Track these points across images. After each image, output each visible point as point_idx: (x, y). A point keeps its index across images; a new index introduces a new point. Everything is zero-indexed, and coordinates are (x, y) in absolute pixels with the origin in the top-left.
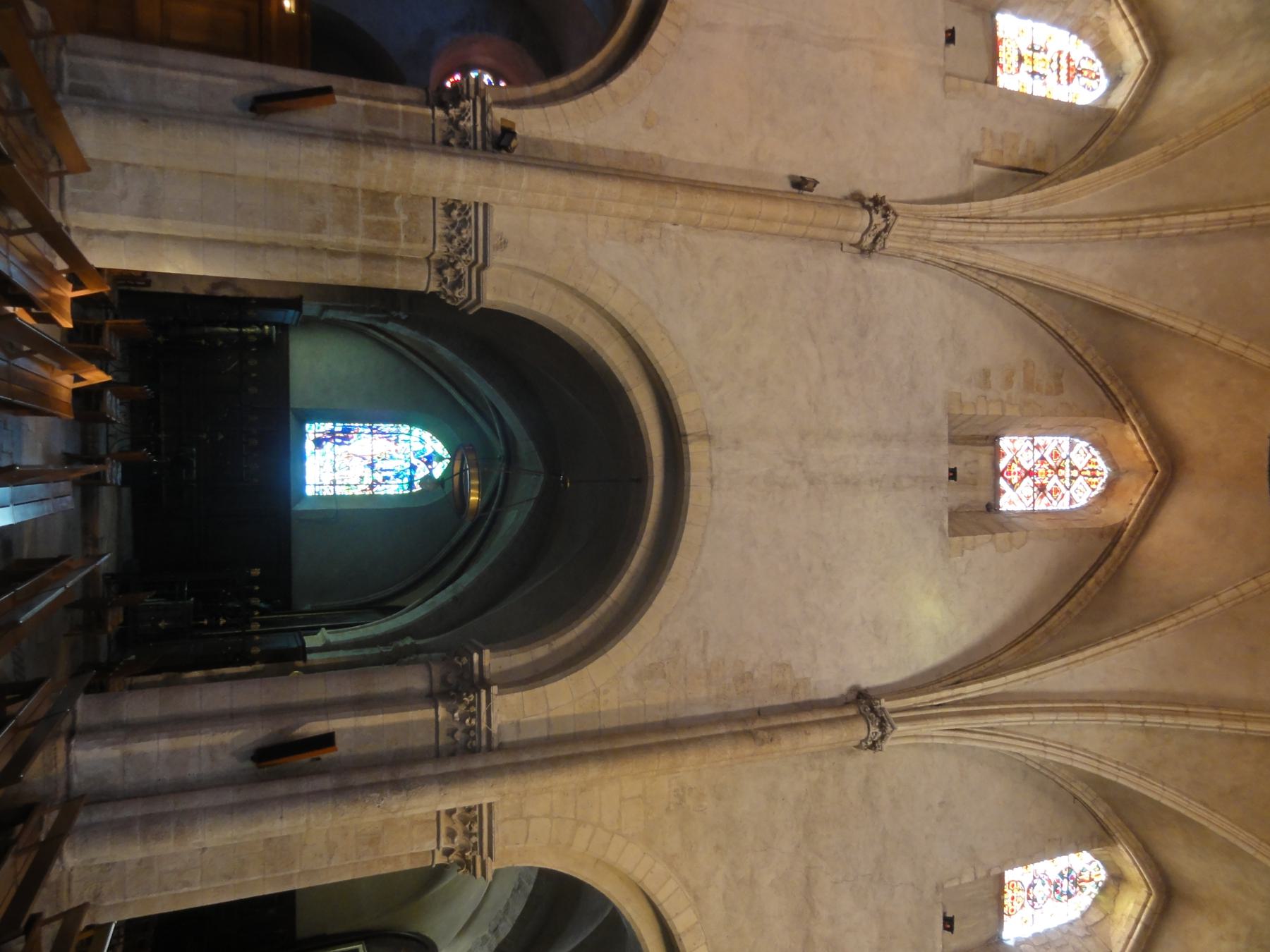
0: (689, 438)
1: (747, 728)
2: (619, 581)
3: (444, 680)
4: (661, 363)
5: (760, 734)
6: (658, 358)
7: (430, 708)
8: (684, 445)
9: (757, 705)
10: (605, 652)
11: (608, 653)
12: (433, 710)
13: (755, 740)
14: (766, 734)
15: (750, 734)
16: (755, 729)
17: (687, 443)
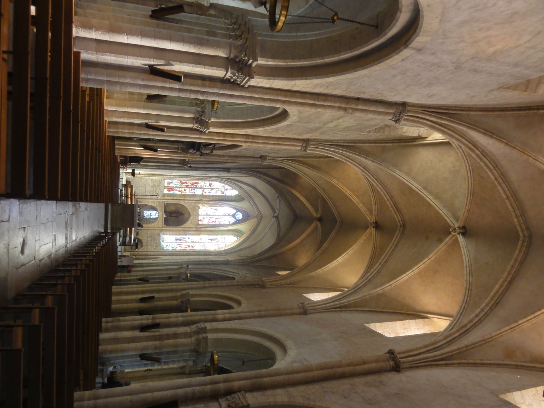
0: (408, 48)
1: (346, 106)
2: (333, 57)
3: (236, 57)
4: (423, 25)
5: (350, 111)
6: (424, 22)
7: (224, 71)
8: (403, 47)
9: (359, 97)
10: (306, 79)
11: (308, 80)
12: (225, 72)
13: (345, 112)
14: (351, 111)
15: (345, 109)
16: (349, 108)
17: (405, 48)
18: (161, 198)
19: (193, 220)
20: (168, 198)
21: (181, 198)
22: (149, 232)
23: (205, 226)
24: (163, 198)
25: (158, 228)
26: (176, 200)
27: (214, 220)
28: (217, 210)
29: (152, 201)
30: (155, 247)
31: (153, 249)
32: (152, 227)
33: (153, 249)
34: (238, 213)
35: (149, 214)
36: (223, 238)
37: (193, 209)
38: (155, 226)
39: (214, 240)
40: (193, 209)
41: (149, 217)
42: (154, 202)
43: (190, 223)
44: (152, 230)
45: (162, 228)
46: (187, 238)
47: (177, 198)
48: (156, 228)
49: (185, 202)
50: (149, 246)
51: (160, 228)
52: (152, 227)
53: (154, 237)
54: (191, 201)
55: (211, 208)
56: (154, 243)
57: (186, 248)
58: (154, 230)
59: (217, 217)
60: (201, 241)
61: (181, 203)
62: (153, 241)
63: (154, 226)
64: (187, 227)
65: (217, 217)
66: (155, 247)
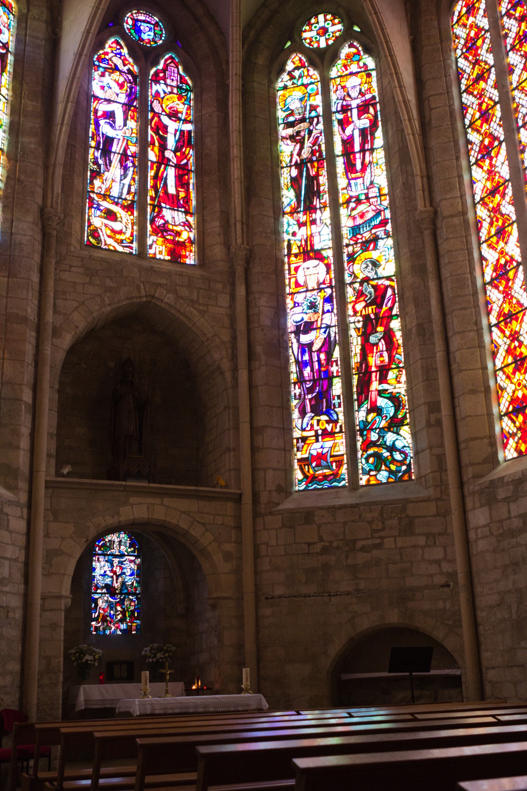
18: (23, 498)
19: (184, 292)
20: (24, 443)
21: (29, 349)
22: (279, 591)
23: (215, 226)
24: (23, 485)
25: (239, 527)
26: (36, 388)
27: (171, 174)
28: (109, 141)
29: (47, 575)
30: (421, 541)
31: (438, 553)
32: (238, 571)
33: (438, 553)
34: (129, 23)
35: (107, 597)
36: (290, 131)
37: (109, 283)
38: (229, 547)
39: (313, 180)
40: (109, 283)
41: (131, 603)
42: (50, 555)
43: (203, 313)
44: (256, 573)
45: (238, 499)
46: (305, 339)
47: (28, 376)
48: (239, 542)
49: (56, 332)
50: (411, 582)
51: (238, 517)
52: (238, 571)
53: (325, 551)
54: (51, 284)
55: (96, 174)
56: (378, 546)
57: (389, 336)
58: (257, 556)
59: (152, 156)
60: (329, 253)
61: (61, 356)
62: (361, 558)
63: (228, 556)
64: (226, 336)
65: (152, 156)
66: (421, 541)
